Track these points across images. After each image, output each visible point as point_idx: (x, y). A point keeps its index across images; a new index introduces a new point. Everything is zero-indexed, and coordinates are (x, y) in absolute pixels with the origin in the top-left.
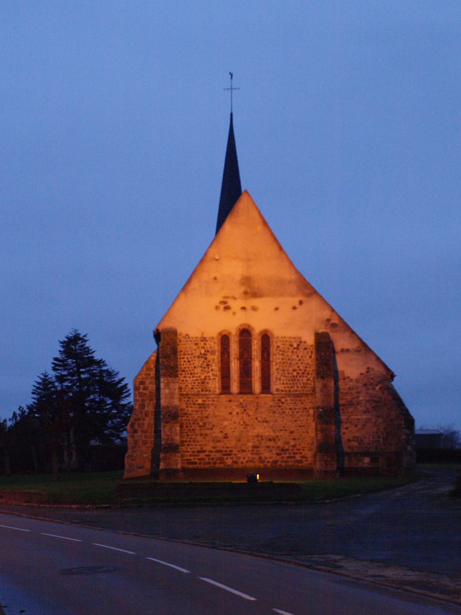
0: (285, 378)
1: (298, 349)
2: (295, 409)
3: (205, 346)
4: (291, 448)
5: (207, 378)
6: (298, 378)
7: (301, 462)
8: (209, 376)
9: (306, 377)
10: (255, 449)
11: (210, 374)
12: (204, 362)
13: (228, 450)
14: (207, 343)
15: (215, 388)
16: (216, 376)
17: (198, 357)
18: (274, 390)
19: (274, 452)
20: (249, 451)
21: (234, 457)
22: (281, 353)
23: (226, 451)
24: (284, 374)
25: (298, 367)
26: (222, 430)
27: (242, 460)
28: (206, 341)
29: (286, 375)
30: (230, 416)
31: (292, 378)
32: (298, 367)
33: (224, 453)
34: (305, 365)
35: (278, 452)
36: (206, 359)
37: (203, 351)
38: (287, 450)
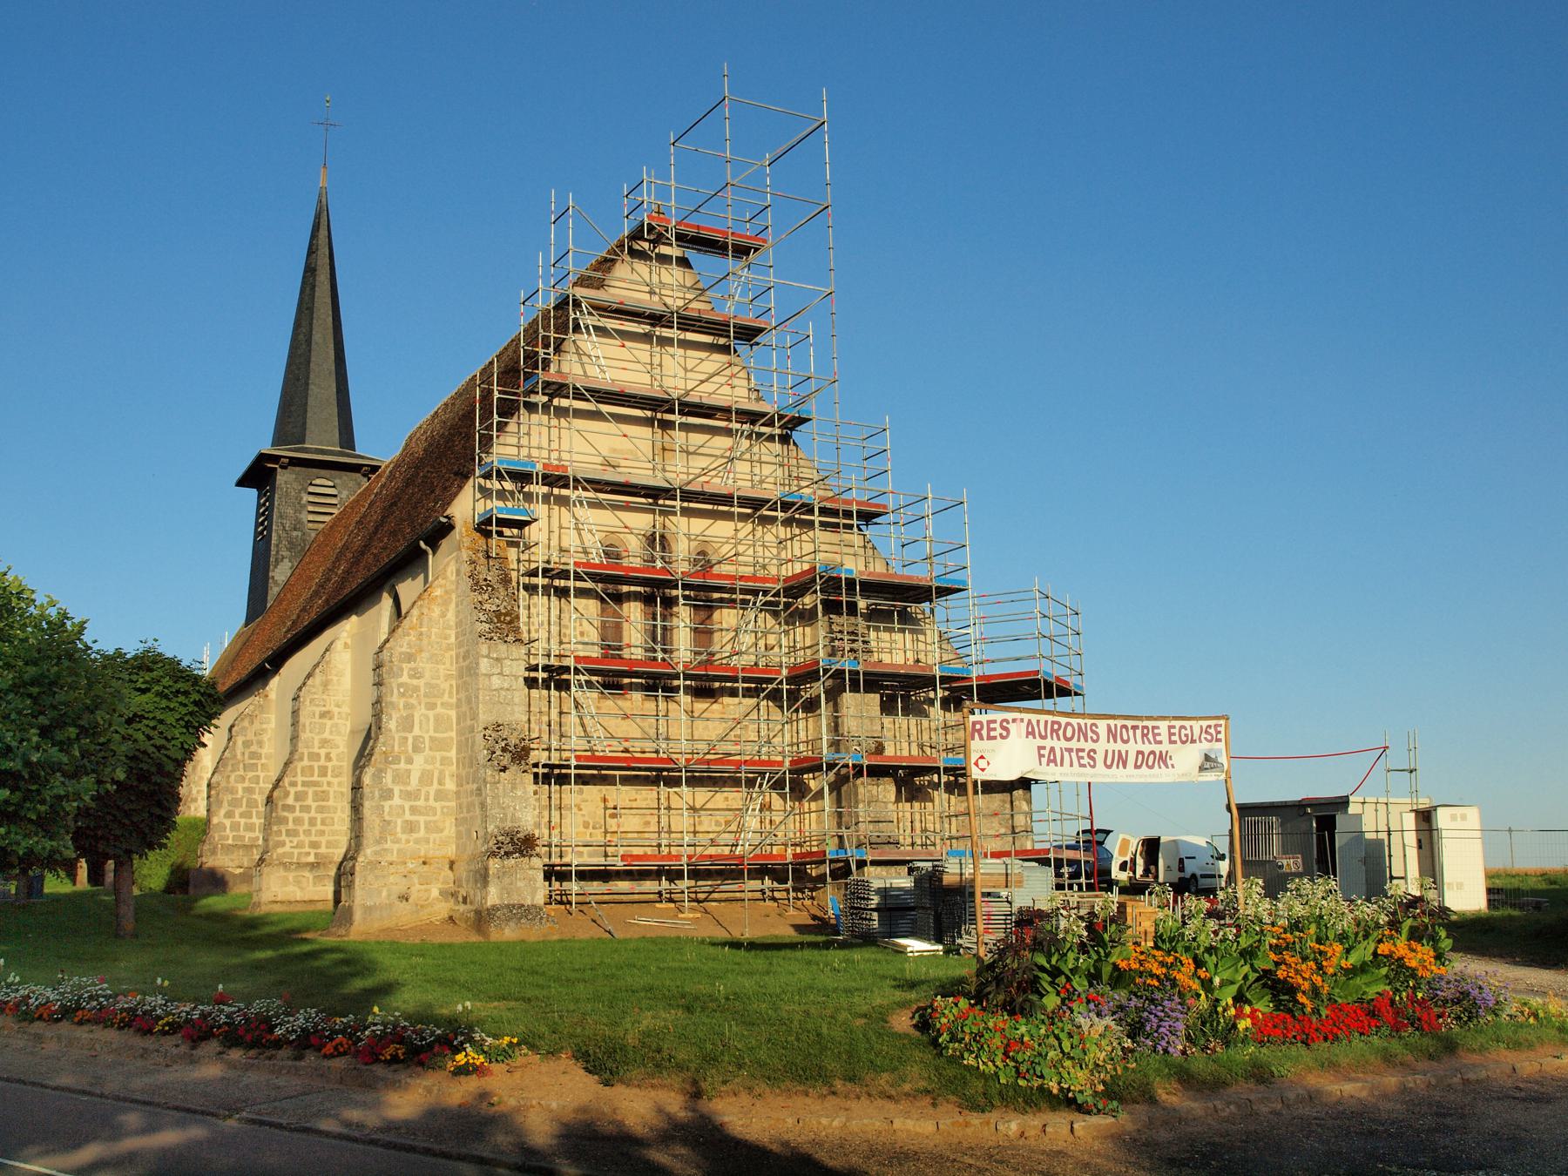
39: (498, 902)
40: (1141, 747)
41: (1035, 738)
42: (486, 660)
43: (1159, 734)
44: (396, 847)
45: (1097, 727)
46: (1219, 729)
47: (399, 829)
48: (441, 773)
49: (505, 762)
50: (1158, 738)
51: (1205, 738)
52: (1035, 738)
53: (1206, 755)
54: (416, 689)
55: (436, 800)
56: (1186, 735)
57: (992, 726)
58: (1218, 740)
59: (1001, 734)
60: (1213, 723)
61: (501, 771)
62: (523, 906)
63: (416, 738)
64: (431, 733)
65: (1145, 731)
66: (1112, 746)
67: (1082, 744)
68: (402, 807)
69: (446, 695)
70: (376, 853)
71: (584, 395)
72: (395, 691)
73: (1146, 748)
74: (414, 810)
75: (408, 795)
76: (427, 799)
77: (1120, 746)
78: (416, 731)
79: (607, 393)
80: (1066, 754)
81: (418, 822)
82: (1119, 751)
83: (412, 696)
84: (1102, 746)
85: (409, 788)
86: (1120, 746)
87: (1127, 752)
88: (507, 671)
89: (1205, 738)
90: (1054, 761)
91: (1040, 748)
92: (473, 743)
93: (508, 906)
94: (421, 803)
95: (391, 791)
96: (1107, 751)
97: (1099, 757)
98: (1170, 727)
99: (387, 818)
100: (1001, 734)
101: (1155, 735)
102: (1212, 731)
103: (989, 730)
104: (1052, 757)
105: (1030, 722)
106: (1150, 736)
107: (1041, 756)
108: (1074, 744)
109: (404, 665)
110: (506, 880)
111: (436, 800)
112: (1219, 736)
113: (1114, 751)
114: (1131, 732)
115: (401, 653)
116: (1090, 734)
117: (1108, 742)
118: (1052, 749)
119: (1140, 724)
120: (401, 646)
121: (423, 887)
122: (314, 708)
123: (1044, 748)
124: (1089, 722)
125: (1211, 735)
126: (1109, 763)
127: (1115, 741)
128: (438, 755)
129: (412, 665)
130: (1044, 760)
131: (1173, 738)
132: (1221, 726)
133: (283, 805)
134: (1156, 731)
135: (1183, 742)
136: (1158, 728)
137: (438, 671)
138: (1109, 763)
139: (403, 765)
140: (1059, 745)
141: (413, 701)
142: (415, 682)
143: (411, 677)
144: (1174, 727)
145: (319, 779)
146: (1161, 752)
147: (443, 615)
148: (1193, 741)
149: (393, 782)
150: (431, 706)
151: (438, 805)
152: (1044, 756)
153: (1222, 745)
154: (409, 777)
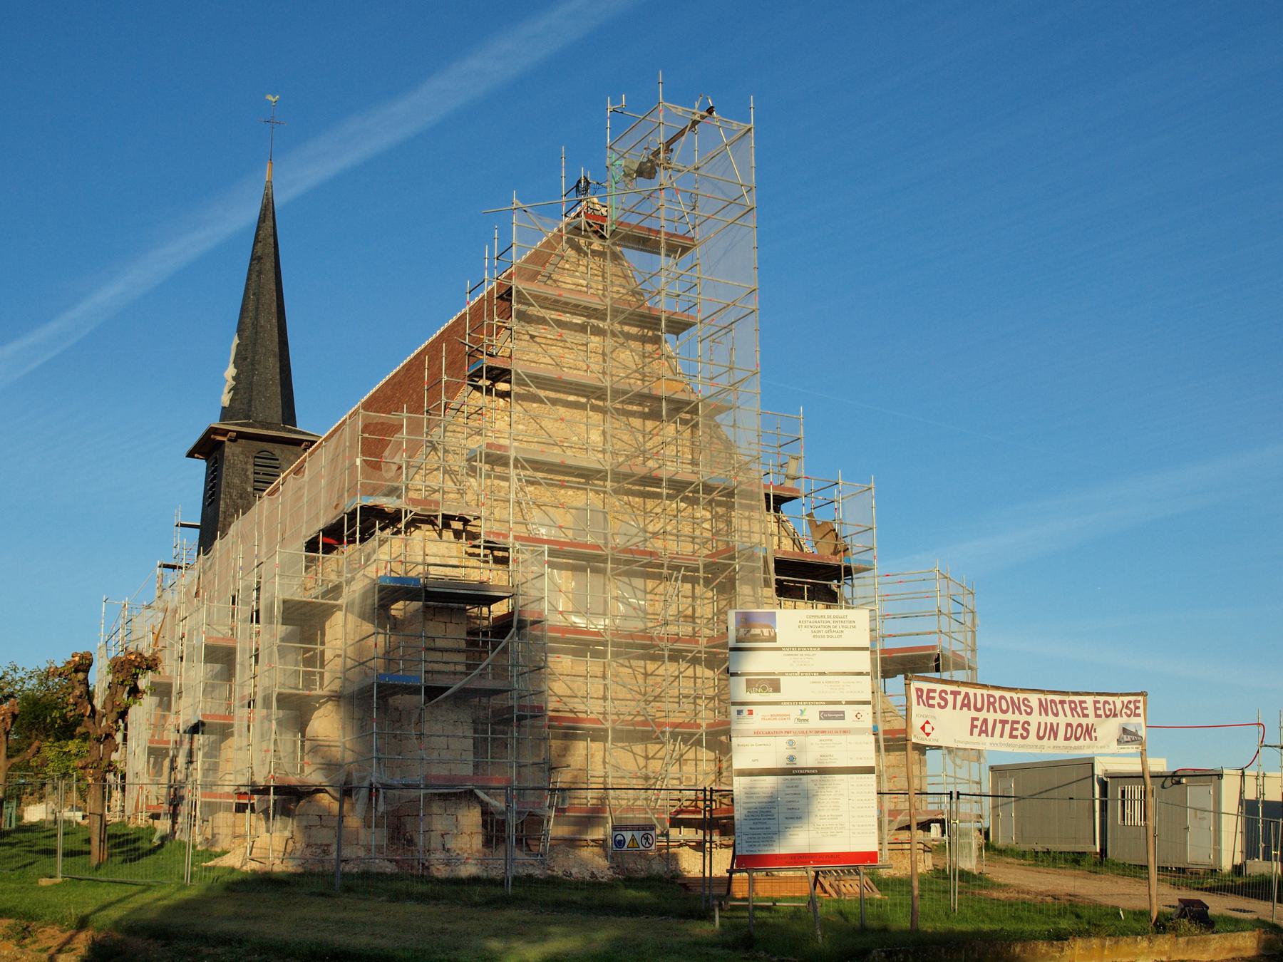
40: (1070, 719)
41: (969, 709)
43: (1086, 708)
45: (1029, 702)
46: (1138, 704)
50: (1086, 712)
51: (1126, 713)
52: (969, 709)
53: (1124, 729)
56: (1110, 710)
57: (932, 695)
58: (1139, 715)
59: (939, 704)
60: (1132, 698)
65: (1073, 705)
66: (1043, 719)
67: (1017, 717)
71: (524, 379)
73: (1075, 721)
77: (1051, 719)
79: (545, 379)
80: (999, 726)
82: (1052, 724)
84: (1035, 719)
86: (1051, 719)
87: (1058, 724)
89: (1126, 713)
90: (986, 732)
91: (974, 719)
96: (1039, 723)
97: (1033, 729)
98: (1096, 702)
100: (939, 704)
101: (1083, 709)
102: (1132, 706)
103: (929, 698)
104: (984, 728)
105: (967, 695)
106: (1079, 709)
107: (973, 726)
108: (1009, 716)
112: (1138, 711)
113: (1046, 723)
114: (1059, 707)
116: (1023, 708)
117: (1041, 715)
118: (985, 721)
119: (1066, 698)
123: (977, 719)
124: (1022, 696)
125: (1131, 710)
126: (1041, 735)
127: (1047, 715)
130: (976, 731)
131: (1099, 712)
132: (1139, 701)
134: (1083, 705)
135: (1107, 716)
136: (1085, 702)
138: (1041, 735)
140: (991, 717)
144: (1098, 702)
146: (1087, 725)
148: (1115, 715)
152: (976, 727)
153: (1141, 720)
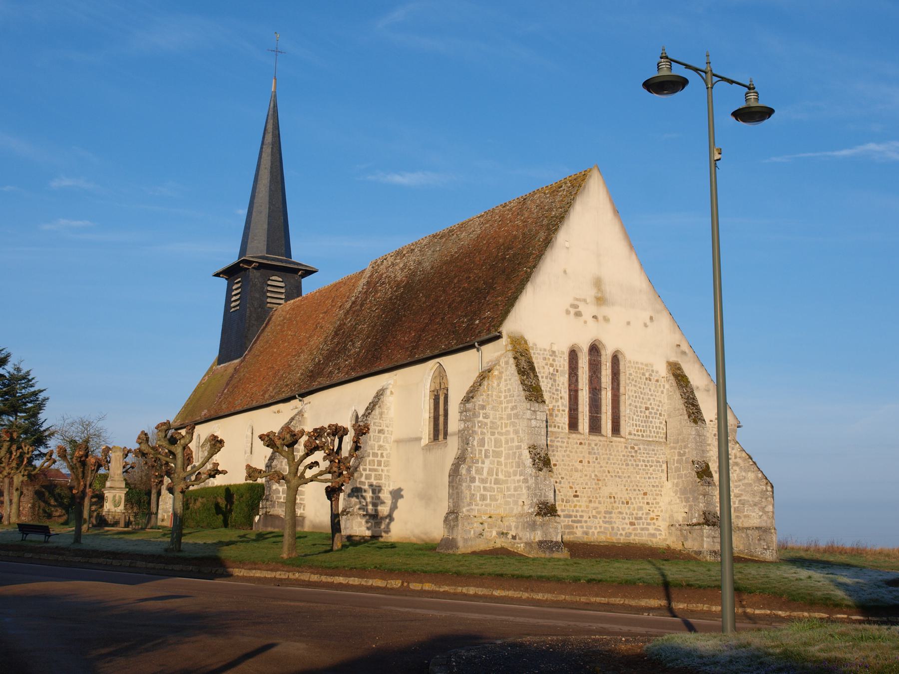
0: (637, 418)
1: (650, 380)
2: (648, 461)
3: (554, 363)
4: (644, 516)
5: (556, 408)
6: (651, 419)
7: (653, 535)
8: (558, 406)
9: (659, 419)
10: (607, 516)
11: (560, 403)
12: (552, 385)
13: (578, 514)
14: (556, 359)
15: (564, 423)
16: (565, 406)
17: (547, 378)
18: (627, 434)
19: (627, 521)
20: (600, 518)
21: (584, 525)
22: (633, 383)
23: (576, 516)
24: (637, 412)
25: (651, 404)
26: (571, 485)
27: (593, 530)
28: (555, 356)
29: (639, 413)
30: (579, 466)
31: (645, 419)
32: (651, 404)
33: (573, 519)
34: (658, 403)
35: (631, 520)
36: (555, 381)
37: (551, 369)
38: (641, 518)
39: (541, 539)
42: (529, 411)
44: (477, 507)
47: (478, 498)
48: (497, 469)
49: (540, 466)
54: (486, 424)
55: (495, 484)
61: (539, 470)
62: (552, 542)
63: (486, 450)
64: (493, 448)
68: (480, 487)
69: (500, 428)
70: (468, 511)
72: (477, 425)
74: (485, 488)
75: (483, 481)
76: (491, 483)
78: (486, 447)
81: (487, 495)
83: (484, 428)
85: (483, 477)
88: (538, 417)
92: (520, 455)
93: (546, 541)
94: (488, 485)
95: (474, 478)
99: (473, 492)
109: (481, 411)
110: (545, 528)
111: (495, 484)
115: (479, 405)
120: (479, 401)
121: (489, 530)
122: (376, 427)
128: (496, 460)
129: (484, 411)
133: (360, 482)
137: (496, 415)
139: (480, 465)
141: (485, 431)
142: (485, 420)
143: (484, 418)
145: (378, 468)
147: (498, 385)
149: (476, 473)
150: (493, 434)
151: (495, 486)
154: (483, 471)
